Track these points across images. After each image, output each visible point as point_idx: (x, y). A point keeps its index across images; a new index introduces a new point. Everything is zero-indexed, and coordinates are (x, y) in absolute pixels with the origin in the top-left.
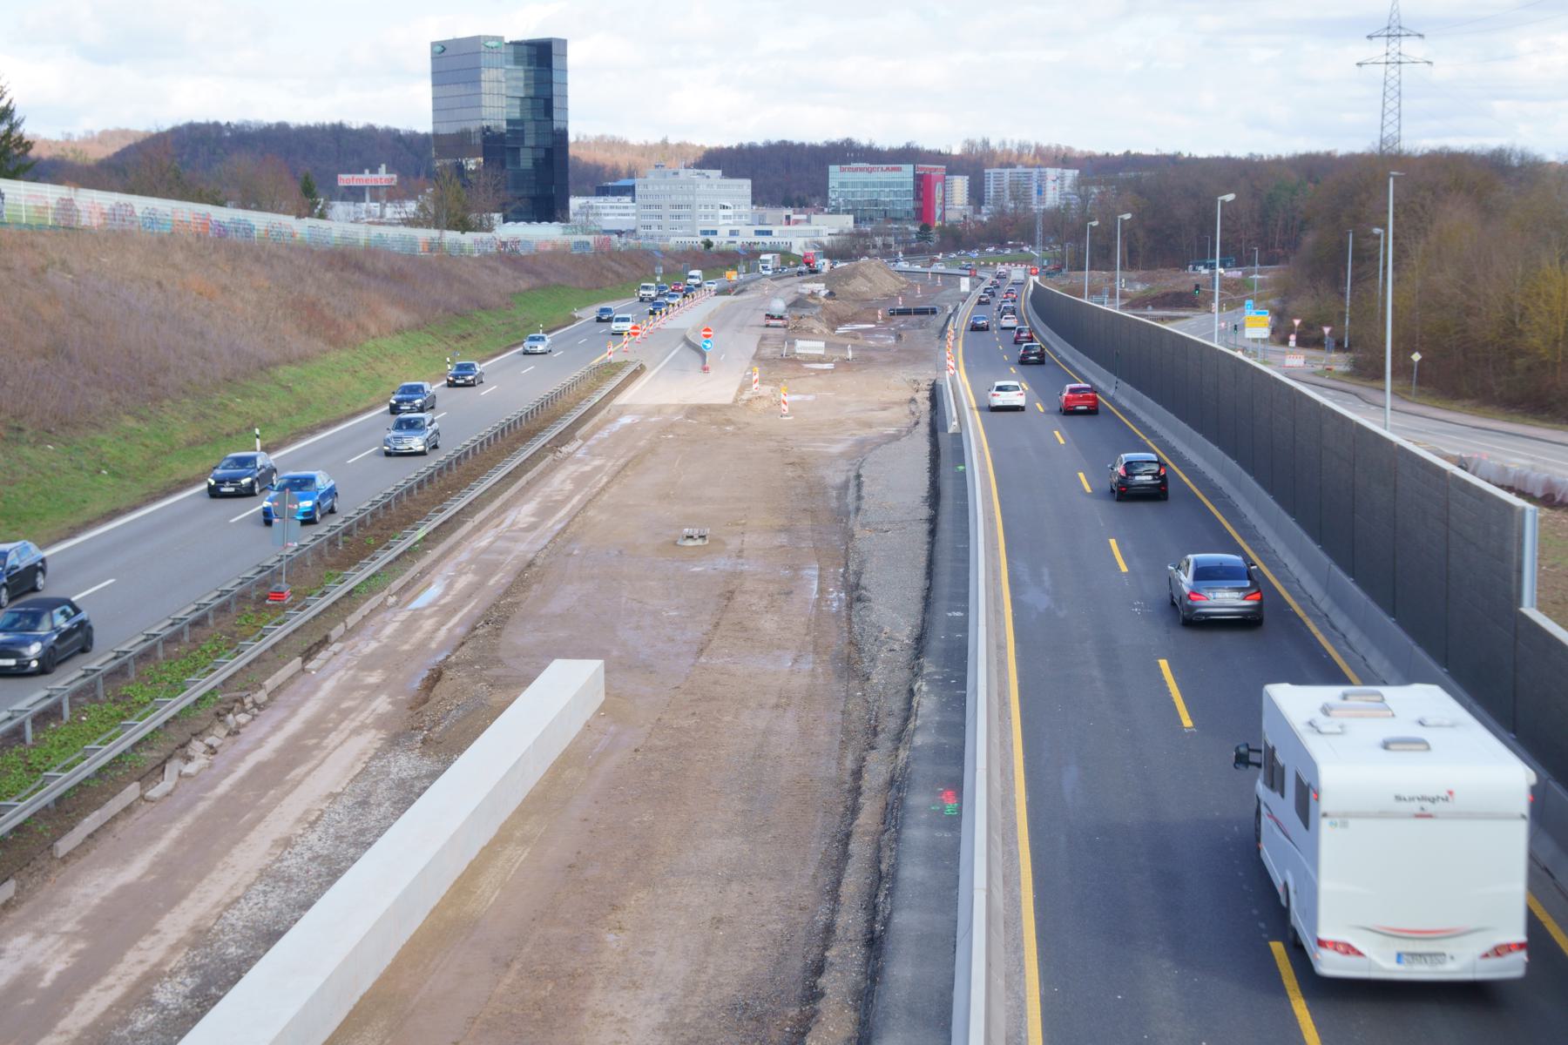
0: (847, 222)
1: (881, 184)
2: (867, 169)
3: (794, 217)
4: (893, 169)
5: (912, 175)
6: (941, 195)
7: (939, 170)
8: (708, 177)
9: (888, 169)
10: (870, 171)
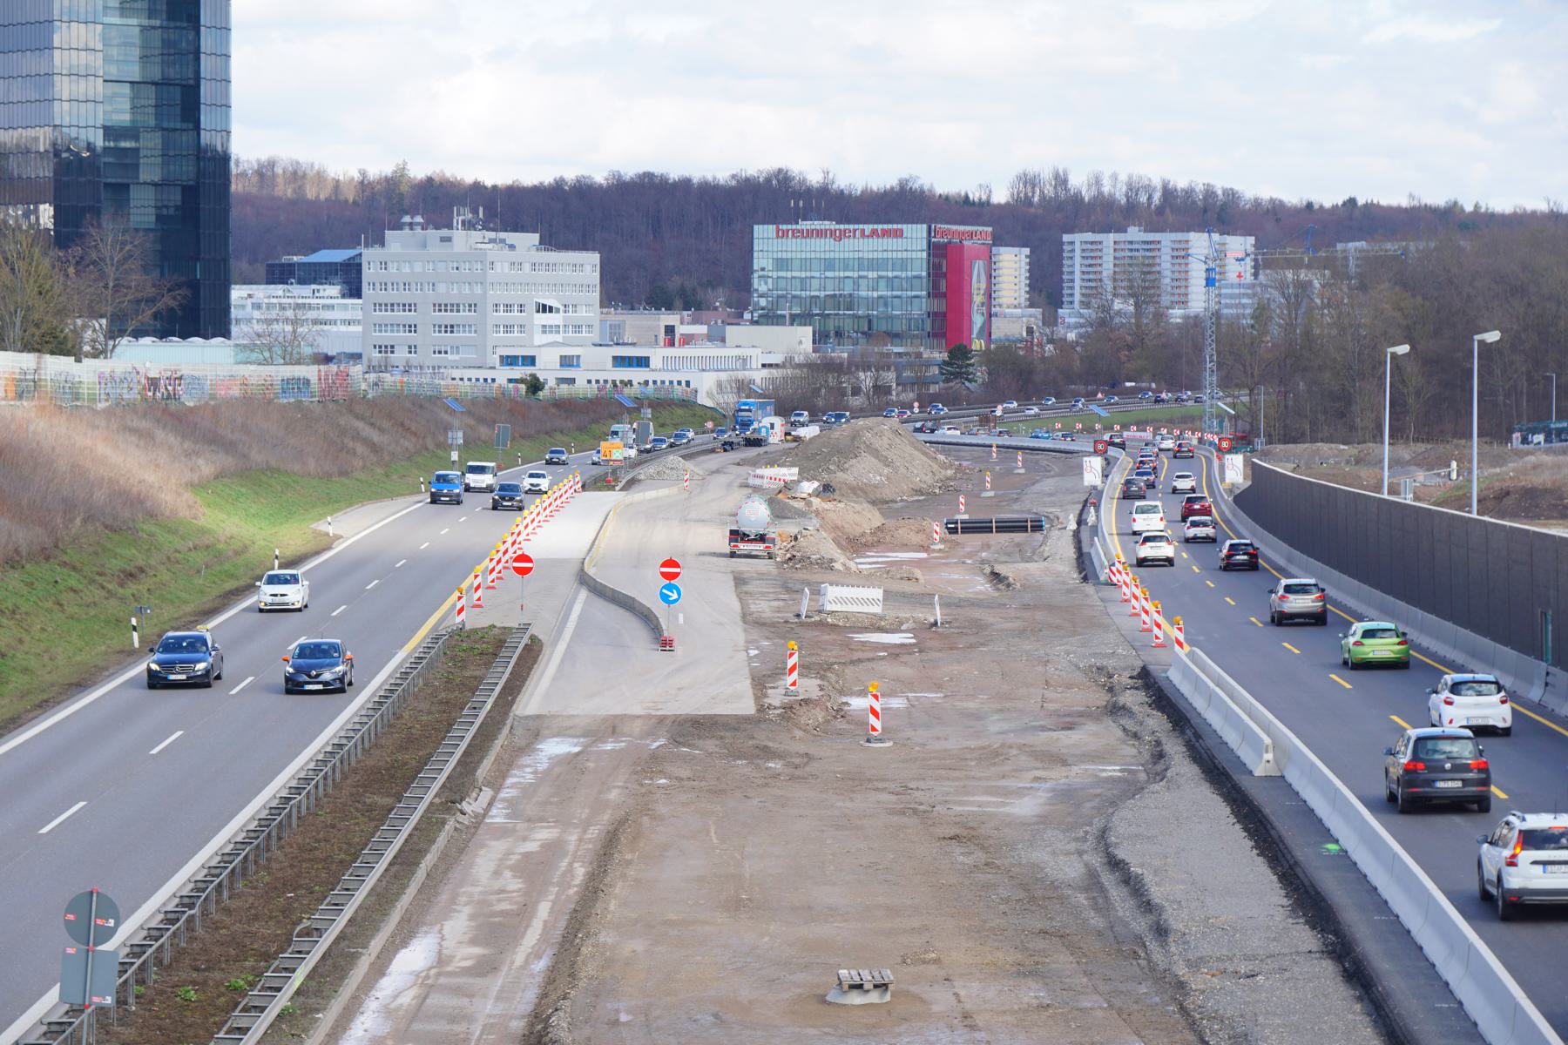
0: (799, 341)
1: (862, 264)
2: (832, 233)
3: (682, 330)
4: (885, 233)
5: (925, 247)
6: (983, 285)
7: (975, 236)
8: (512, 247)
9: (874, 232)
10: (839, 236)
